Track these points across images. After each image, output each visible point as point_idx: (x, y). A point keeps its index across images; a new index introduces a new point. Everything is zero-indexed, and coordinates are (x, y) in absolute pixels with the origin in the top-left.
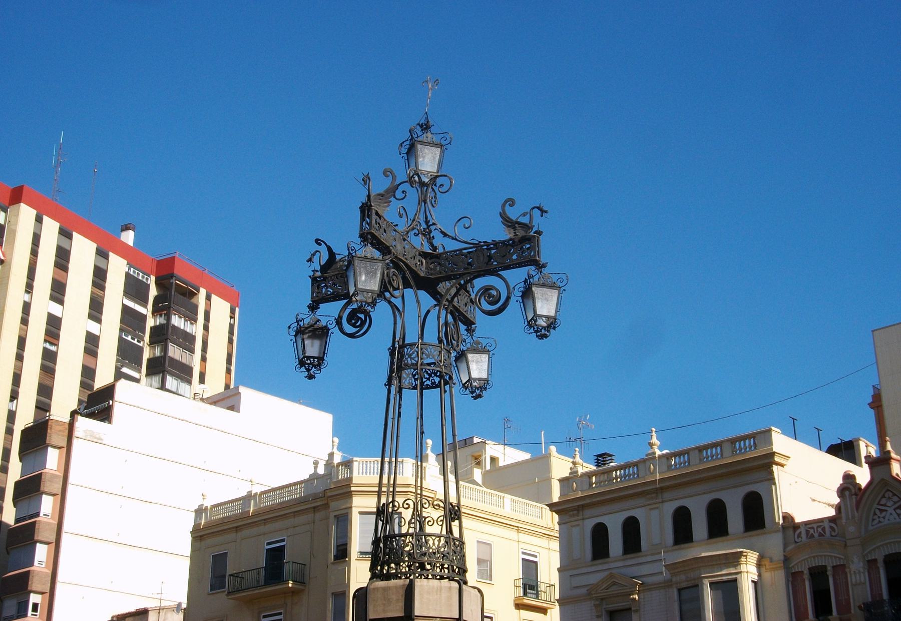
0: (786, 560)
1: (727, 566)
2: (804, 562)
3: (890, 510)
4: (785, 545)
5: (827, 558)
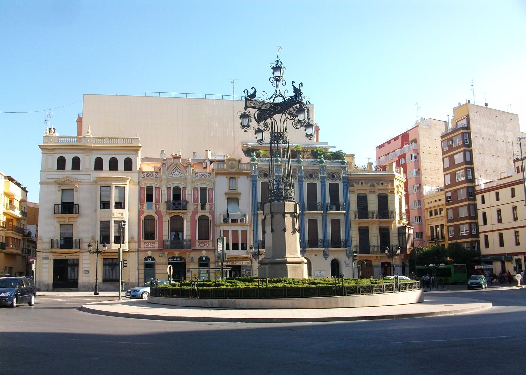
0: (139, 182)
1: (122, 181)
2: (145, 184)
3: (177, 173)
5: (154, 184)
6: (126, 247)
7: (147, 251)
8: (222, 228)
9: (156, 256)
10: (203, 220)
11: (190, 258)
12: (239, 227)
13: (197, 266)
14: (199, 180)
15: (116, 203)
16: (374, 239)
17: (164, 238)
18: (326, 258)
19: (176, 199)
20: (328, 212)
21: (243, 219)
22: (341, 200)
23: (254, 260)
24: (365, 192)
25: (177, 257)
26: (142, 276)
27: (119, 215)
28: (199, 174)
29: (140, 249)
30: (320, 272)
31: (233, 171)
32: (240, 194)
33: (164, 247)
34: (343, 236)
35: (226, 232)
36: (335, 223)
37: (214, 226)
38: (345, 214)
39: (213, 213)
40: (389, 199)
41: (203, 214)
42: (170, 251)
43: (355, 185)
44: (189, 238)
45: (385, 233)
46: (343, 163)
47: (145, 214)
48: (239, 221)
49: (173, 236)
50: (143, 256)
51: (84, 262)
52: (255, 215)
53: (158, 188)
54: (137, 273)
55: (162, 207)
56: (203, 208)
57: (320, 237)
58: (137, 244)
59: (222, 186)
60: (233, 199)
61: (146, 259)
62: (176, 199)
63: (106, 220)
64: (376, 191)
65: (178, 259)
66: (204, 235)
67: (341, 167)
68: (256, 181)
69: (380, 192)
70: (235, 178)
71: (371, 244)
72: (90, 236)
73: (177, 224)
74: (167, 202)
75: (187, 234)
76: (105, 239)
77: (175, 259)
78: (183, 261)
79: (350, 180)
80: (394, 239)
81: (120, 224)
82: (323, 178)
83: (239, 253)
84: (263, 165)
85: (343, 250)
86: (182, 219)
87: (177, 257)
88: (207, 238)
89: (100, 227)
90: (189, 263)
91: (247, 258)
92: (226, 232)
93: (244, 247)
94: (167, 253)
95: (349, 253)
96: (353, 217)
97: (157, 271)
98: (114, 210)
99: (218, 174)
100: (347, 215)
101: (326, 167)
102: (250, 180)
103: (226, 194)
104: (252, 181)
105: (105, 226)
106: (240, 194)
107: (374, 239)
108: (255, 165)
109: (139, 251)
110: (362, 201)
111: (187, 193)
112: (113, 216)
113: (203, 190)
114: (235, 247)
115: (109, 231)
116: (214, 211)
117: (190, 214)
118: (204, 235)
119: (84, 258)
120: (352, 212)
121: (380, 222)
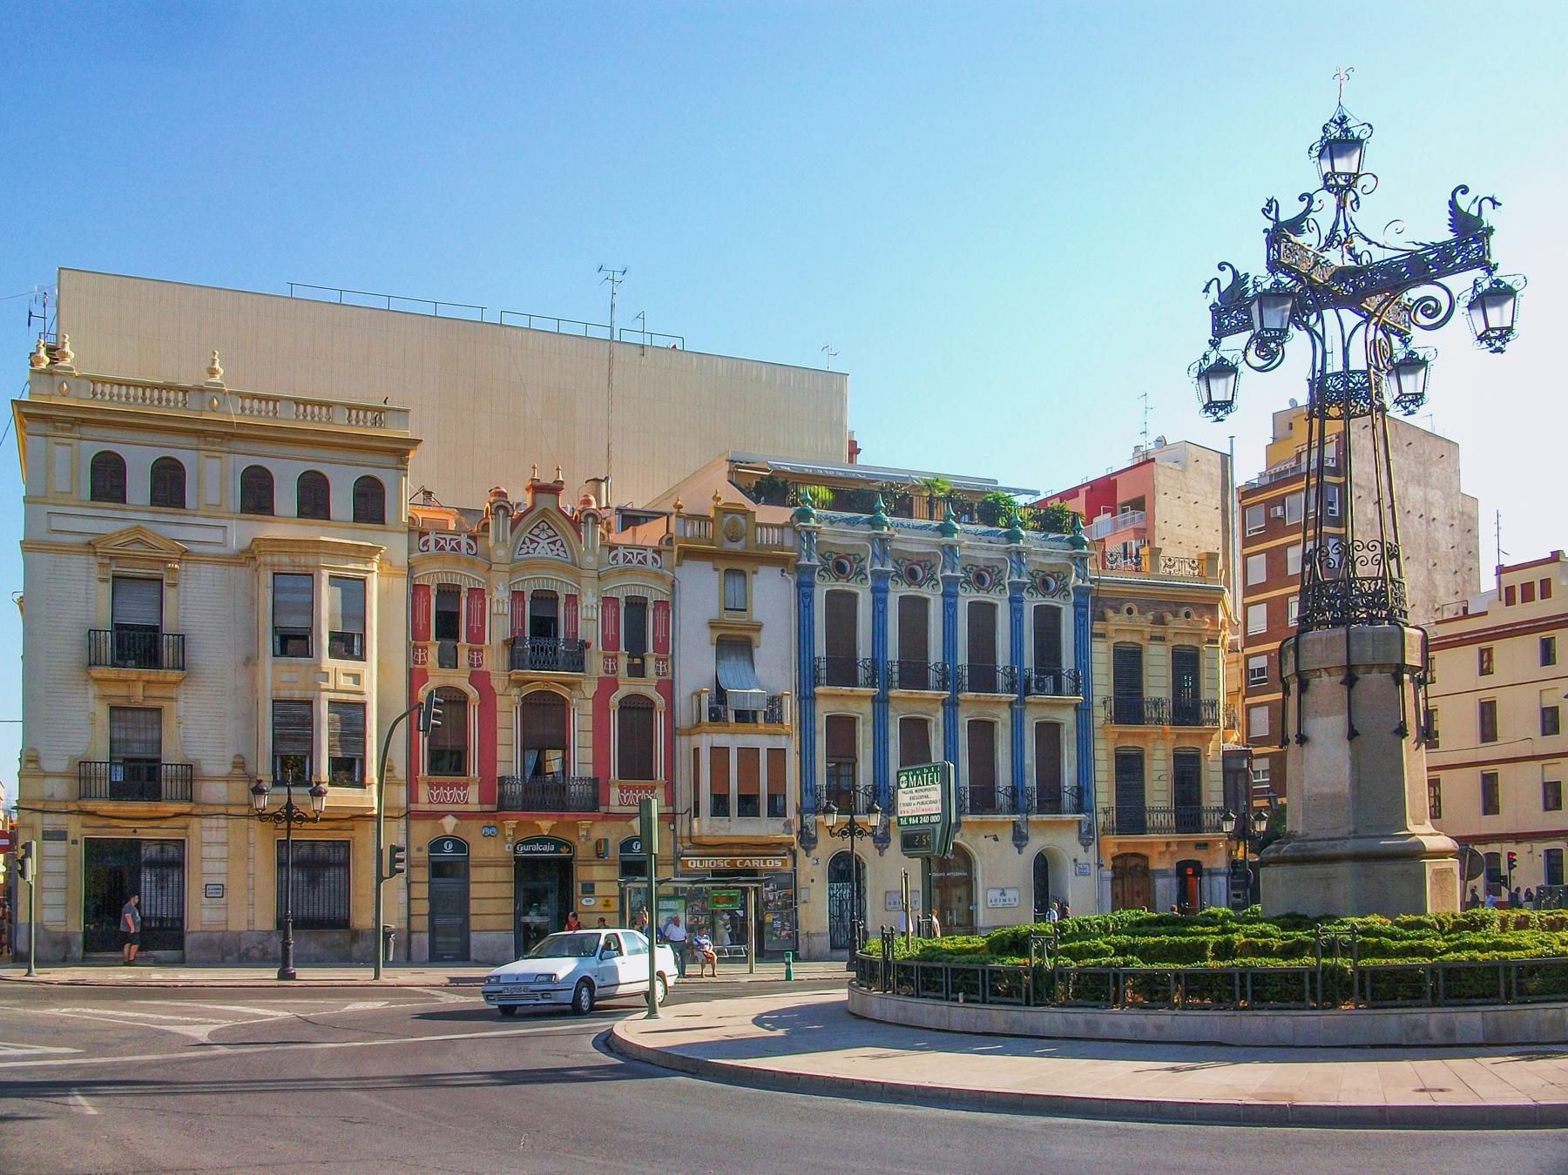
4: (410, 551)
6: (367, 798)
7: (443, 814)
8: (706, 742)
9: (473, 834)
10: (637, 711)
11: (593, 842)
12: (763, 743)
13: (614, 873)
14: (623, 572)
15: (334, 636)
16: (1158, 791)
17: (501, 770)
18: (1020, 848)
19: (543, 630)
20: (1029, 699)
21: (772, 711)
22: (1068, 661)
23: (801, 853)
24: (1136, 639)
25: (543, 840)
26: (423, 907)
27: (345, 683)
28: (621, 551)
29: (413, 807)
30: (1003, 894)
31: (737, 547)
32: (758, 628)
33: (499, 803)
34: (1069, 776)
35: (719, 753)
36: (1049, 734)
37: (672, 732)
38: (1077, 707)
39: (667, 688)
40: (1204, 663)
41: (634, 690)
42: (525, 816)
43: (1110, 613)
44: (589, 771)
45: (1187, 770)
46: (1076, 543)
47: (433, 683)
48: (761, 719)
49: (531, 763)
50: (424, 832)
51: (206, 851)
52: (806, 699)
53: (477, 593)
54: (403, 896)
55: (494, 661)
56: (637, 671)
57: (1004, 778)
58: (403, 791)
59: (700, 595)
60: (735, 643)
61: (436, 845)
62: (543, 630)
63: (297, 695)
64: (1170, 637)
65: (546, 848)
66: (637, 765)
67: (1072, 558)
68: (812, 585)
69: (1178, 641)
70: (742, 573)
71: (1148, 804)
72: (229, 755)
73: (545, 721)
74: (512, 644)
75: (582, 761)
76: (293, 766)
77: (537, 847)
78: (564, 853)
79: (1096, 600)
80: (1213, 791)
81: (350, 714)
82: (1017, 588)
83: (763, 828)
84: (835, 534)
85: (1071, 822)
86: (563, 704)
87: (543, 840)
88: (648, 774)
89: (274, 724)
90: (588, 863)
91: (780, 845)
92: (719, 753)
93: (776, 810)
94: (511, 823)
95: (1089, 832)
96: (1100, 715)
97: (475, 890)
98: (328, 663)
99: (687, 554)
100: (1083, 711)
101: (1029, 552)
102: (792, 580)
103: (713, 625)
104: (799, 585)
105: (293, 719)
106: (758, 628)
107: (1158, 791)
108: (809, 533)
109: (411, 815)
110: (1128, 663)
111: (583, 613)
112: (324, 685)
113: (636, 607)
114: (748, 805)
115: (309, 740)
116: (672, 682)
117: (590, 689)
118: (637, 765)
119: (206, 836)
120: (1097, 701)
121: (1178, 735)
